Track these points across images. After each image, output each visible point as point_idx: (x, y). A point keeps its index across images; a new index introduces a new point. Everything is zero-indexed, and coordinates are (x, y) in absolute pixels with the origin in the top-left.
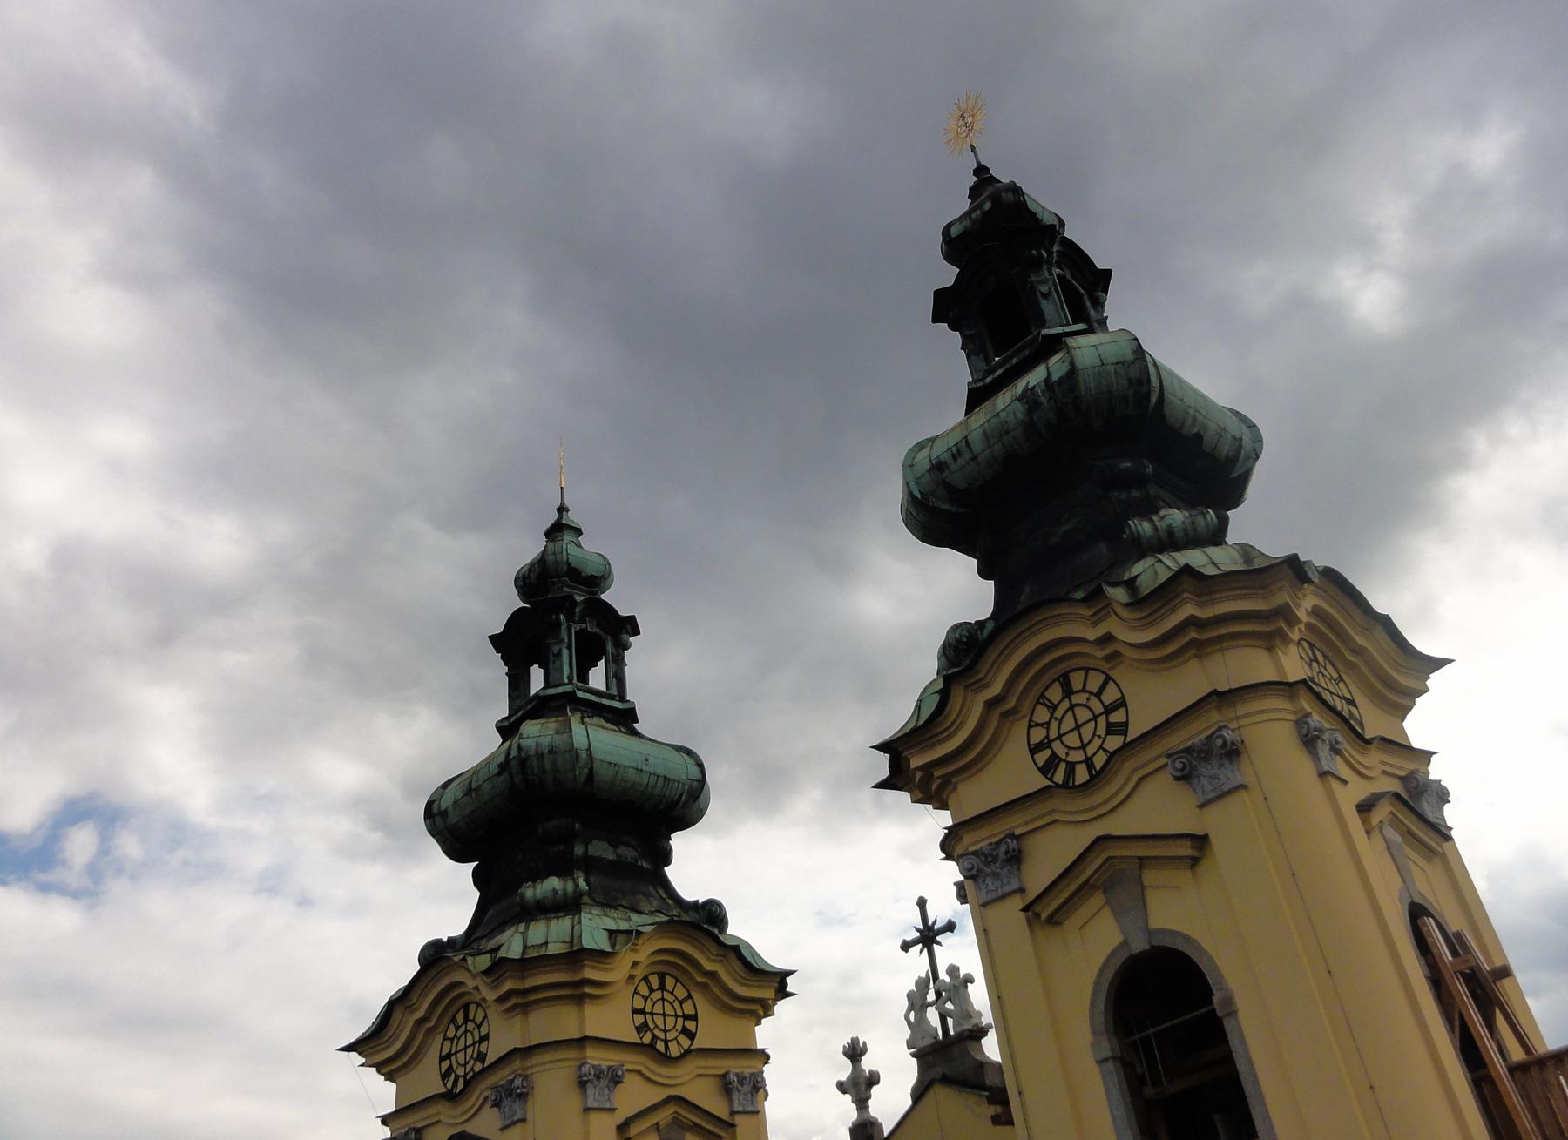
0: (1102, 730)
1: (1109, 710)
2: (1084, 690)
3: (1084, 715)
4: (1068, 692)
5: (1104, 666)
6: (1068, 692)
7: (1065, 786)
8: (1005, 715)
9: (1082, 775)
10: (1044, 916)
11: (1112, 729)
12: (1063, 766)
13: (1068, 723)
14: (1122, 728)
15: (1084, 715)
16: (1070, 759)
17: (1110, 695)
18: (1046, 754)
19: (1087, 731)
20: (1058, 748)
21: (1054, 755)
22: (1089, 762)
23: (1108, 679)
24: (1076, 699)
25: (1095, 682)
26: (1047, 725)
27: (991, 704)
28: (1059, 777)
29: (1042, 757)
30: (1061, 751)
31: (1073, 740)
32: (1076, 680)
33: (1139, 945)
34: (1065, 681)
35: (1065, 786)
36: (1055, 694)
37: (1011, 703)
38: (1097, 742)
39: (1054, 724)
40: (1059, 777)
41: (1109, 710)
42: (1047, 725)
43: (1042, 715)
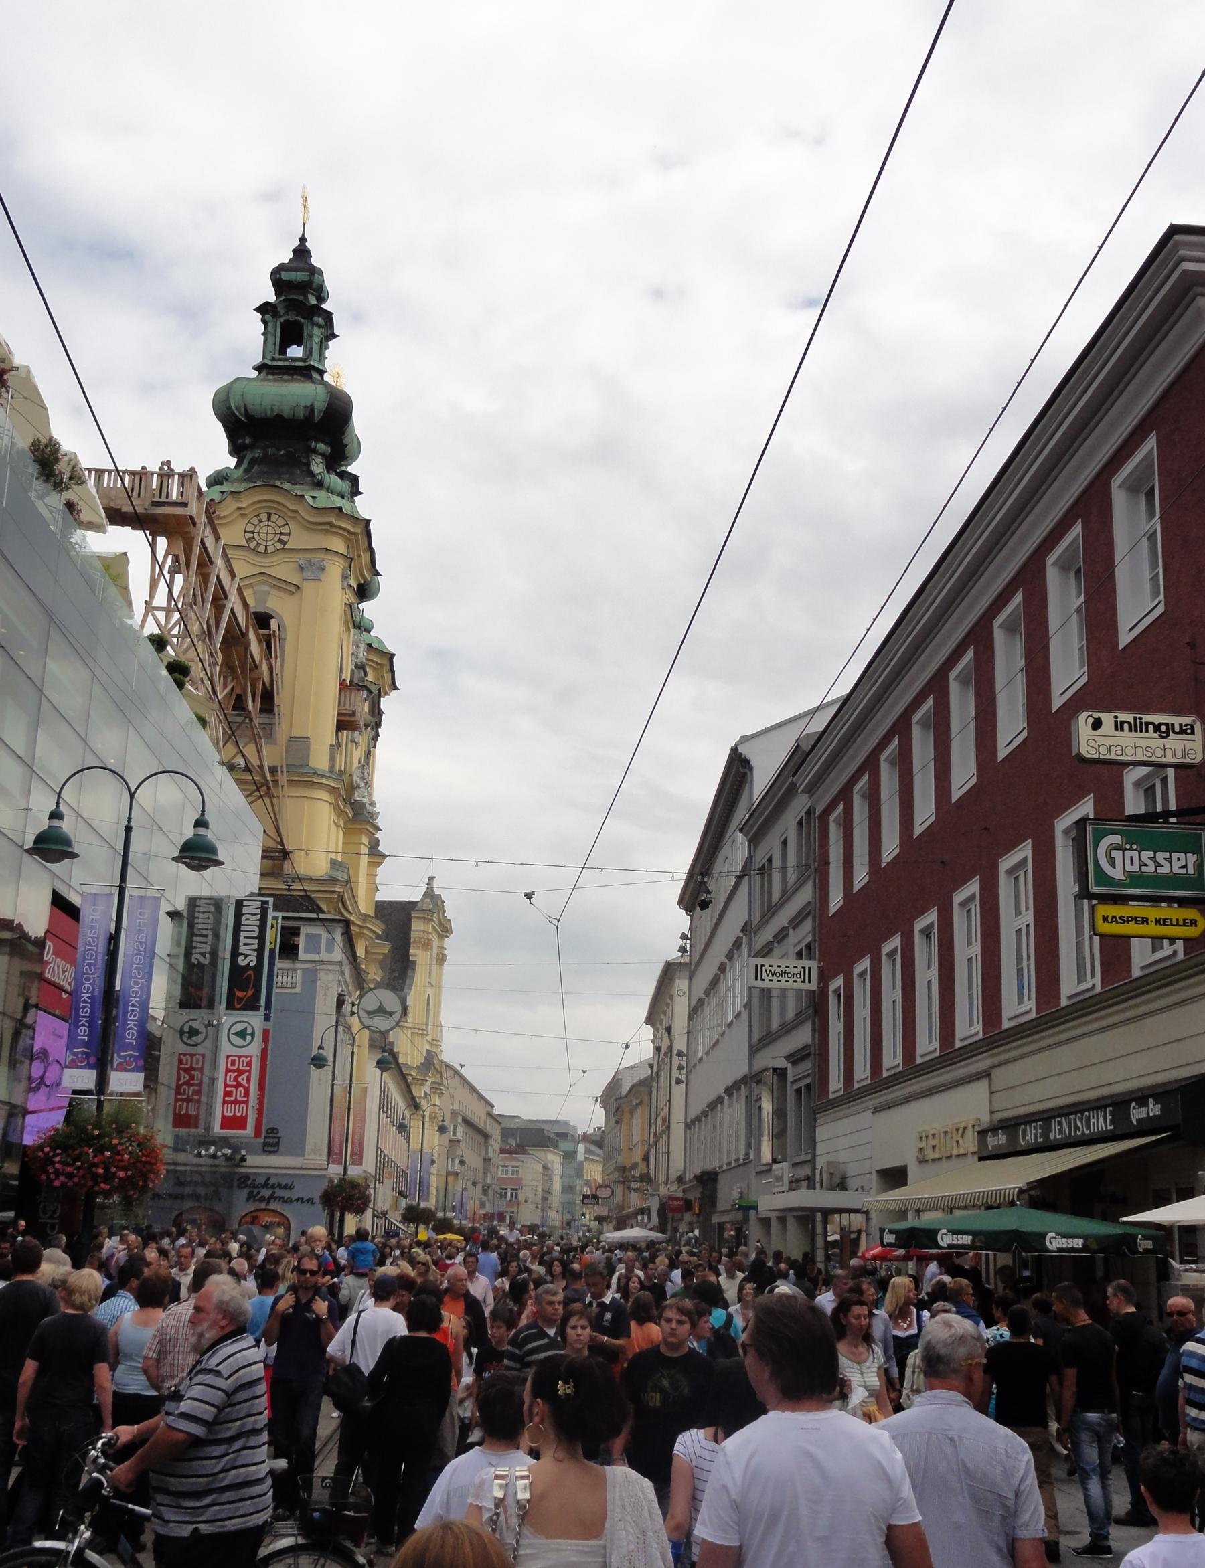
0: (276, 539)
1: (282, 534)
3: (271, 530)
4: (269, 520)
6: (269, 520)
7: (254, 550)
8: (241, 514)
11: (280, 541)
12: (255, 543)
13: (264, 530)
14: (284, 543)
15: (271, 530)
20: (256, 535)
21: (253, 538)
22: (266, 546)
23: (287, 524)
26: (256, 525)
27: (239, 508)
28: (252, 545)
29: (249, 536)
31: (264, 536)
32: (274, 518)
34: (269, 514)
35: (254, 550)
36: (264, 517)
38: (273, 542)
39: (258, 527)
40: (252, 545)
41: (282, 534)
42: (256, 525)
43: (255, 521)
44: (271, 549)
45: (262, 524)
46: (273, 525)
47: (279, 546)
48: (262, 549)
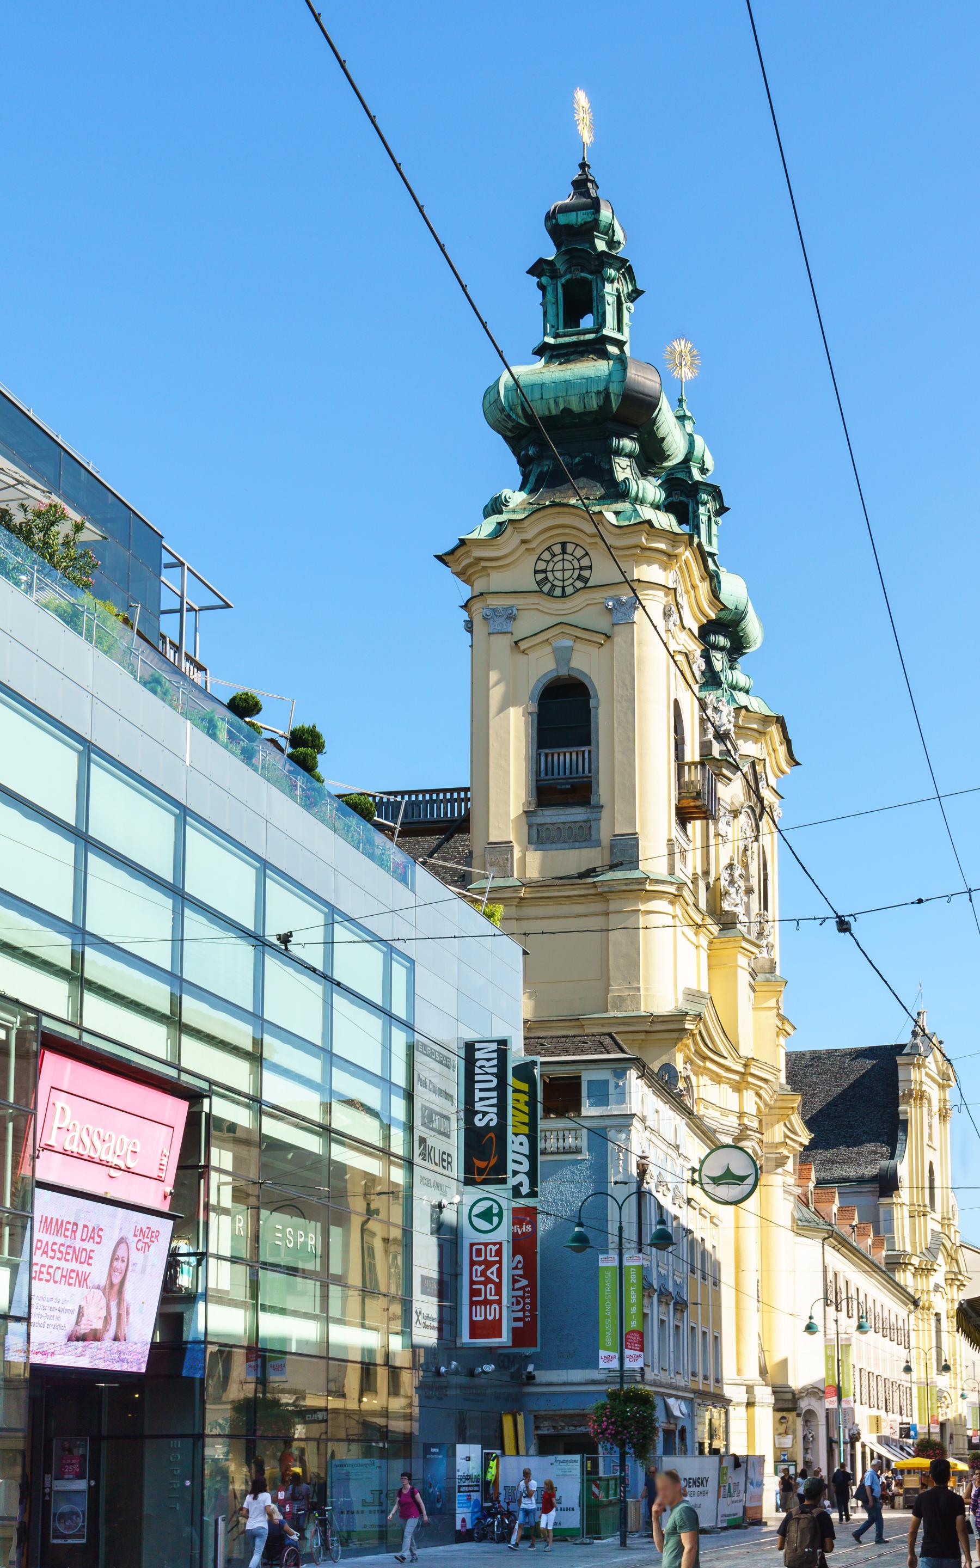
0: (575, 576)
2: (572, 555)
3: (568, 565)
5: (587, 548)
9: (558, 592)
10: (522, 648)
12: (549, 585)
13: (559, 566)
15: (568, 565)
16: (554, 583)
17: (585, 562)
18: (543, 576)
19: (568, 574)
21: (546, 578)
22: (563, 588)
24: (566, 557)
25: (579, 553)
29: (540, 576)
30: (551, 577)
33: (563, 672)
37: (533, 545)
40: (546, 588)
41: (581, 568)
43: (547, 556)
44: (569, 590)
45: (556, 559)
46: (570, 558)
47: (579, 584)
48: (558, 592)
